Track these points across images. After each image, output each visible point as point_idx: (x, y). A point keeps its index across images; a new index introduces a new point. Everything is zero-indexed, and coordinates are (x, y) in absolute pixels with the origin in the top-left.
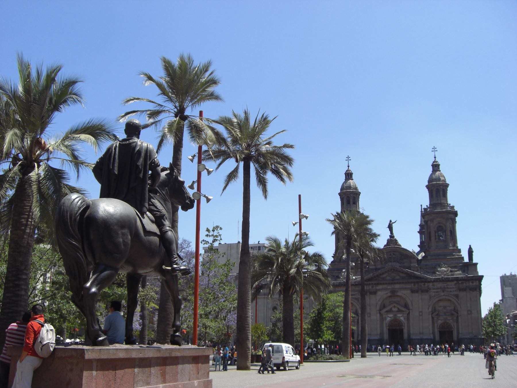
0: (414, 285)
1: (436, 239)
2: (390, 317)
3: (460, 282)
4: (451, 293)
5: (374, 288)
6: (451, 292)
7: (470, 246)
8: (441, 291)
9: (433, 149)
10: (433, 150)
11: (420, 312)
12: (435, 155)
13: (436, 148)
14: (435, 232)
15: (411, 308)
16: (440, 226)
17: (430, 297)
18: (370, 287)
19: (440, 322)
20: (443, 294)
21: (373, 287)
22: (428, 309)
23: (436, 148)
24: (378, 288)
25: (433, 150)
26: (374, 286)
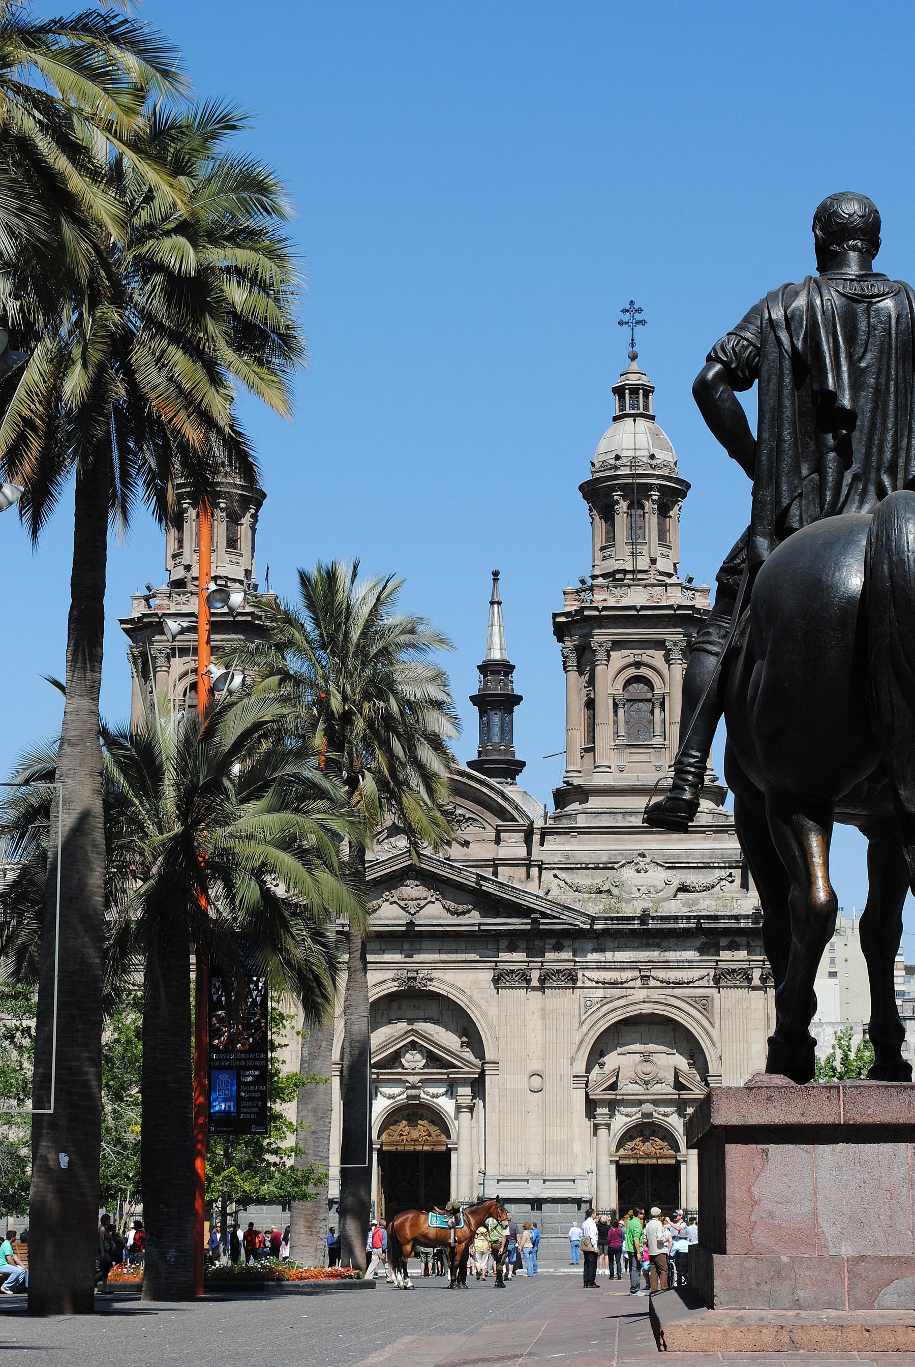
1: (616, 734)
2: (390, 1097)
3: (723, 942)
6: (679, 984)
9: (625, 311)
10: (626, 317)
12: (633, 340)
13: (639, 310)
14: (615, 705)
19: (621, 1122)
20: (642, 994)
22: (573, 1060)
23: (639, 310)
25: (626, 317)
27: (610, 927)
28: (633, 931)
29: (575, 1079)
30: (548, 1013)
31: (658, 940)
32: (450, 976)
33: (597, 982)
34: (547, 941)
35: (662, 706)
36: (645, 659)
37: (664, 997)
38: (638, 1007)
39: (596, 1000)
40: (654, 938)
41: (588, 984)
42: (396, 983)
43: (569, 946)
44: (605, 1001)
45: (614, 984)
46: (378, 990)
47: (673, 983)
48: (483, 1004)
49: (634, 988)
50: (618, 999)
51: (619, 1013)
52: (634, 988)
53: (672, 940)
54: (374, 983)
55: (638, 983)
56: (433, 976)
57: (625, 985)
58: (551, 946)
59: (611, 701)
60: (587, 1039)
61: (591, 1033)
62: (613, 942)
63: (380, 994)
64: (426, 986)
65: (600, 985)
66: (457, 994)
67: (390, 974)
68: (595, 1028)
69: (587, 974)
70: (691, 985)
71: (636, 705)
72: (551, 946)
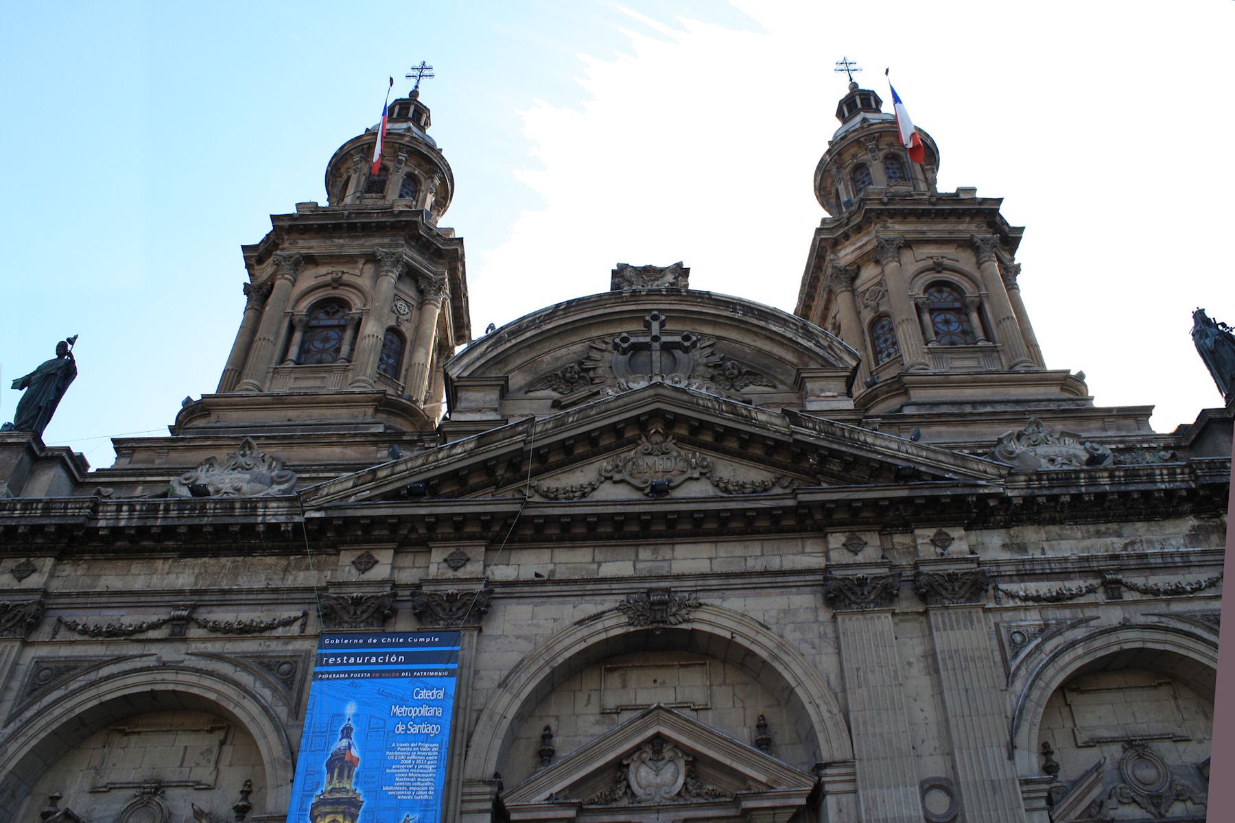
0: (853, 546)
4: (1178, 607)
5: (473, 569)
6: (1177, 592)
7: (1200, 316)
8: (1091, 590)
11: (928, 786)
15: (831, 746)
16: (939, 285)
17: (1010, 645)
18: (435, 563)
20: (1114, 616)
21: (456, 562)
22: (1012, 748)
24: (502, 572)
26: (477, 553)
27: (1037, 492)
28: (1076, 497)
29: (1025, 788)
30: (944, 659)
31: (1114, 526)
32: (735, 603)
33: (1026, 598)
34: (917, 532)
35: (980, 310)
36: (946, 262)
37: (1155, 619)
38: (1113, 638)
39: (1031, 630)
40: (1106, 522)
41: (1011, 604)
42: (624, 619)
43: (961, 539)
44: (1047, 633)
45: (1058, 599)
46: (585, 632)
47: (1165, 593)
48: (805, 648)
49: (1096, 605)
50: (1073, 626)
51: (1080, 650)
52: (1096, 605)
53: (1139, 525)
54: (576, 620)
55: (1100, 596)
56: (701, 601)
57: (1082, 600)
58: (926, 540)
59: (912, 303)
60: (1030, 705)
61: (1035, 694)
62: (1038, 533)
63: (591, 641)
64: (688, 621)
65: (1031, 603)
66: (752, 634)
67: (610, 603)
68: (1041, 684)
69: (1002, 586)
70: (1197, 594)
71: (942, 316)
72: (926, 540)
